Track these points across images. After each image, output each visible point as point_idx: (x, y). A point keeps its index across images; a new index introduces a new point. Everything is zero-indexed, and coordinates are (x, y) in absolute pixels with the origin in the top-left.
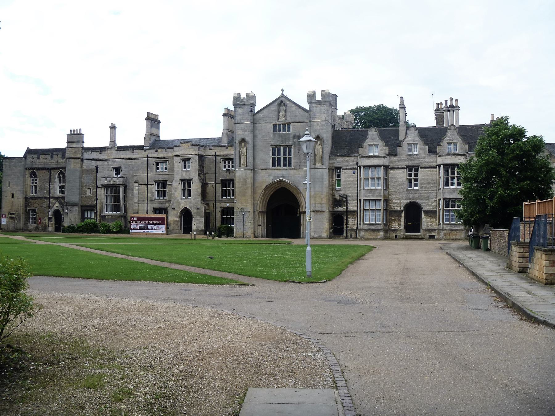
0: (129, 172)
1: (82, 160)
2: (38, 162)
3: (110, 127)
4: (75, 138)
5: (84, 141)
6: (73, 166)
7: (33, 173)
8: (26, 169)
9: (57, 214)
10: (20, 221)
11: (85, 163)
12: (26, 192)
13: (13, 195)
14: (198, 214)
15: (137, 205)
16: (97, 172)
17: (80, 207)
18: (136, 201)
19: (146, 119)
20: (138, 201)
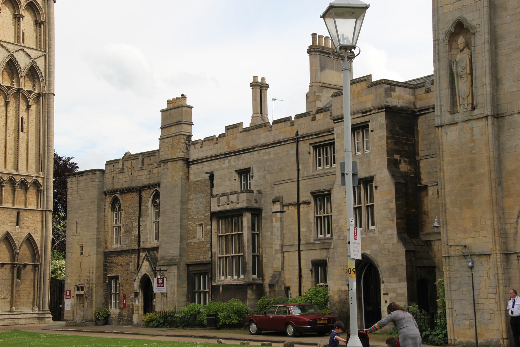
0: (264, 177)
1: (188, 163)
2: (120, 176)
3: (252, 85)
4: (176, 115)
5: (194, 120)
6: (171, 177)
7: (115, 201)
8: (105, 193)
9: (146, 284)
10: (92, 302)
11: (193, 168)
12: (106, 242)
13: (82, 247)
14: (393, 270)
15: (279, 256)
16: (212, 186)
17: (183, 267)
18: (278, 247)
19: (310, 51)
20: (282, 246)
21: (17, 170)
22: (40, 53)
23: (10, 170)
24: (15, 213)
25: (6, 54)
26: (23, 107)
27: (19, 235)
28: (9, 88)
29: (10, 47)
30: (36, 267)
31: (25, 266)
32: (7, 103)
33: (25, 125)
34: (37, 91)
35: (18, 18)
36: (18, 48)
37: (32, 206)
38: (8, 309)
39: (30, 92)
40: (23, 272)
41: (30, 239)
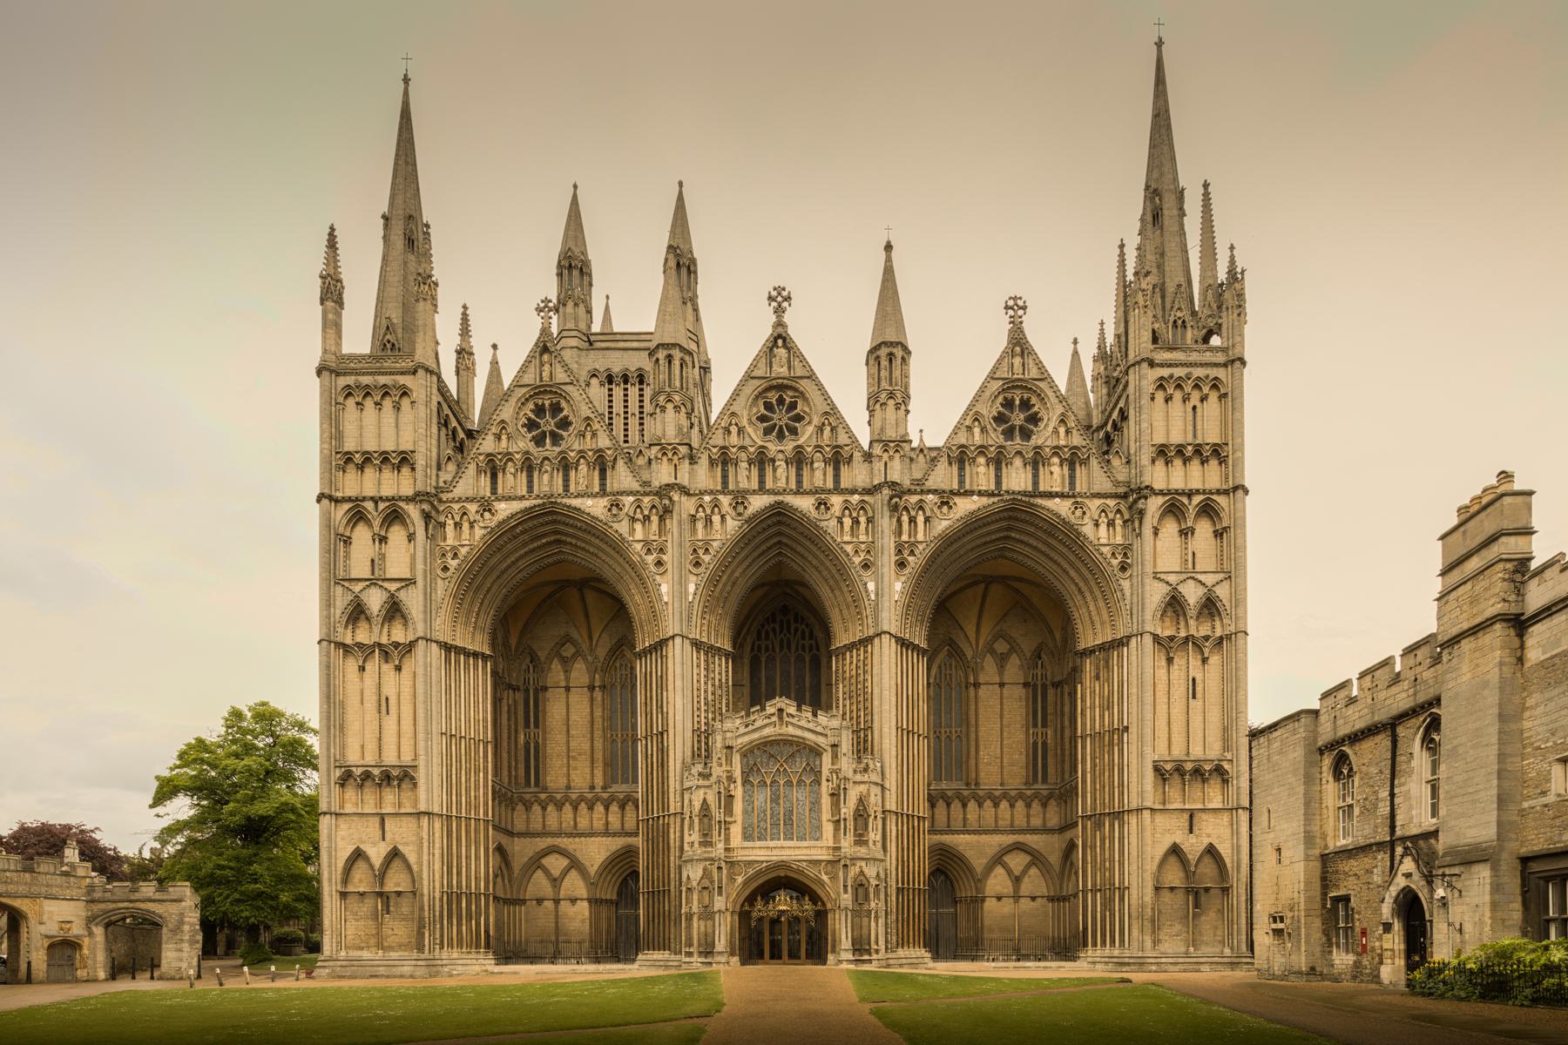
21: (1188, 754)
22: (1222, 576)
23: (1178, 752)
24: (1186, 816)
25: (1165, 589)
26: (1195, 662)
27: (1193, 846)
28: (1171, 638)
29: (1172, 579)
30: (1225, 891)
31: (1207, 890)
32: (1170, 661)
33: (1199, 689)
34: (1218, 633)
35: (1185, 533)
36: (1184, 576)
37: (1216, 804)
38: (1183, 949)
39: (1207, 638)
40: (1203, 898)
41: (1211, 851)
